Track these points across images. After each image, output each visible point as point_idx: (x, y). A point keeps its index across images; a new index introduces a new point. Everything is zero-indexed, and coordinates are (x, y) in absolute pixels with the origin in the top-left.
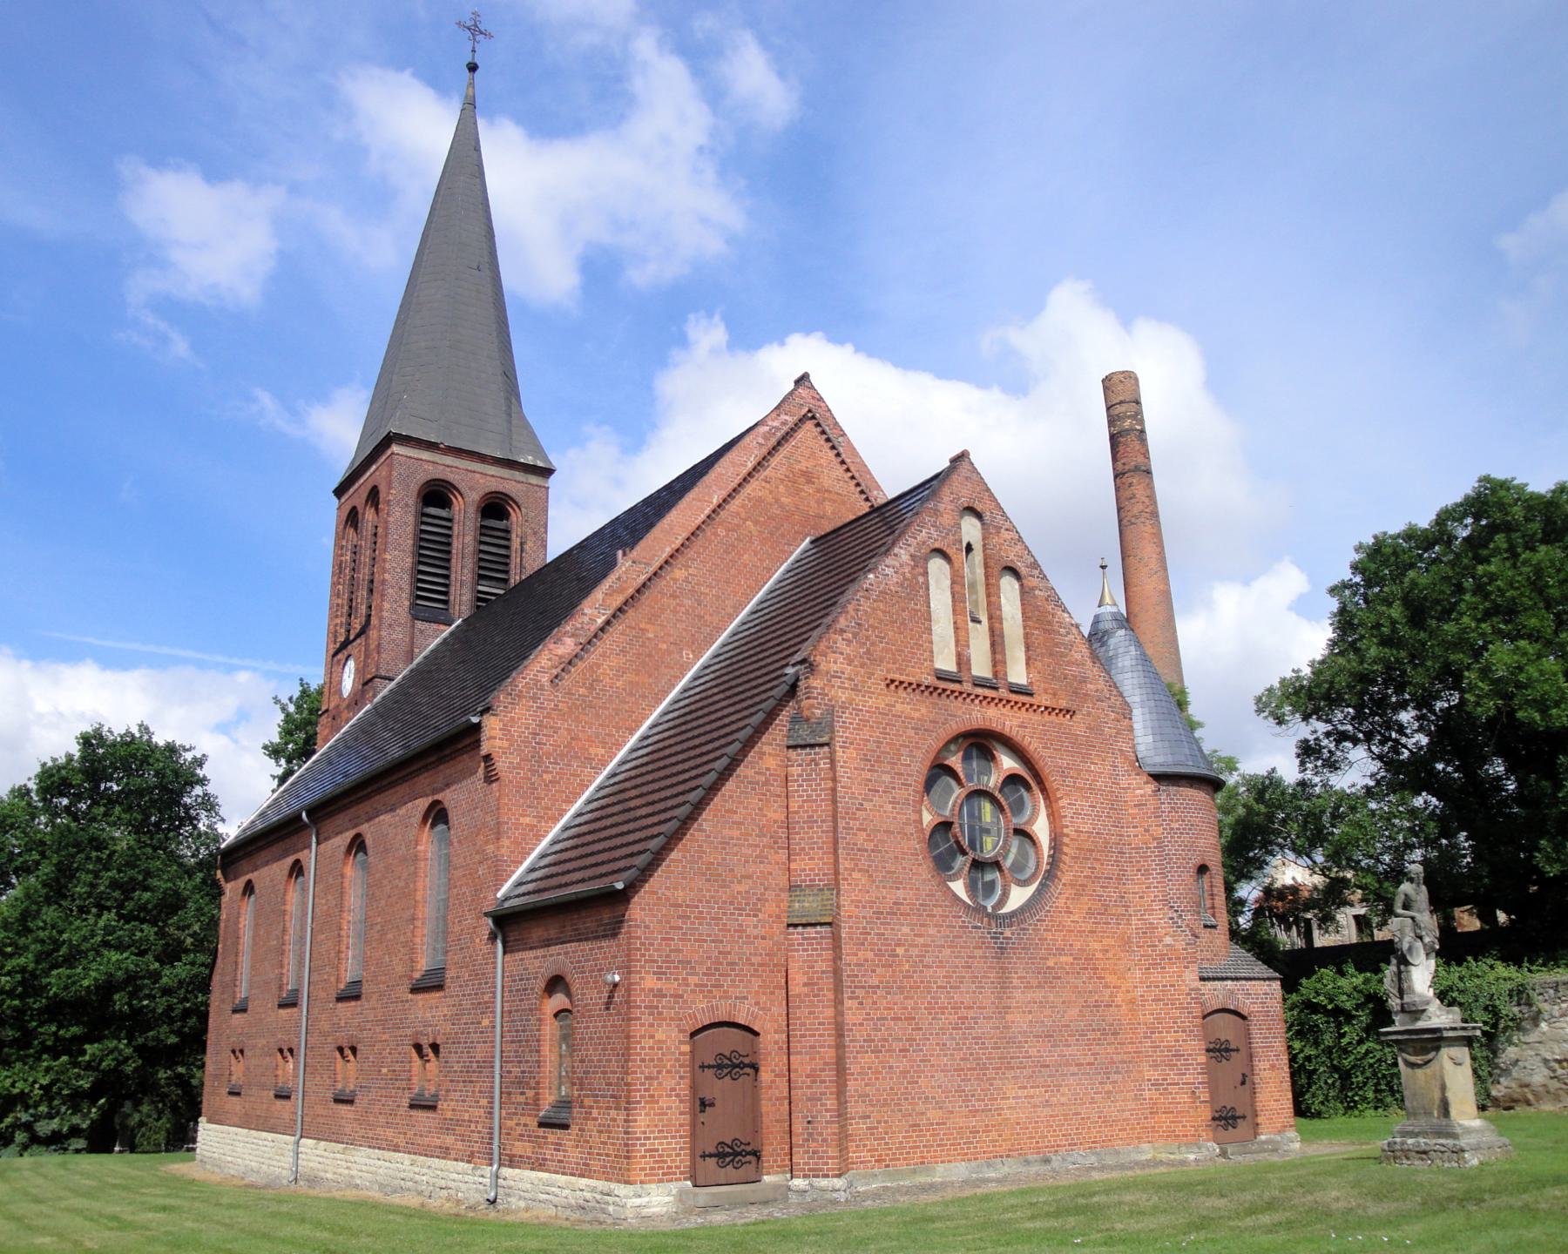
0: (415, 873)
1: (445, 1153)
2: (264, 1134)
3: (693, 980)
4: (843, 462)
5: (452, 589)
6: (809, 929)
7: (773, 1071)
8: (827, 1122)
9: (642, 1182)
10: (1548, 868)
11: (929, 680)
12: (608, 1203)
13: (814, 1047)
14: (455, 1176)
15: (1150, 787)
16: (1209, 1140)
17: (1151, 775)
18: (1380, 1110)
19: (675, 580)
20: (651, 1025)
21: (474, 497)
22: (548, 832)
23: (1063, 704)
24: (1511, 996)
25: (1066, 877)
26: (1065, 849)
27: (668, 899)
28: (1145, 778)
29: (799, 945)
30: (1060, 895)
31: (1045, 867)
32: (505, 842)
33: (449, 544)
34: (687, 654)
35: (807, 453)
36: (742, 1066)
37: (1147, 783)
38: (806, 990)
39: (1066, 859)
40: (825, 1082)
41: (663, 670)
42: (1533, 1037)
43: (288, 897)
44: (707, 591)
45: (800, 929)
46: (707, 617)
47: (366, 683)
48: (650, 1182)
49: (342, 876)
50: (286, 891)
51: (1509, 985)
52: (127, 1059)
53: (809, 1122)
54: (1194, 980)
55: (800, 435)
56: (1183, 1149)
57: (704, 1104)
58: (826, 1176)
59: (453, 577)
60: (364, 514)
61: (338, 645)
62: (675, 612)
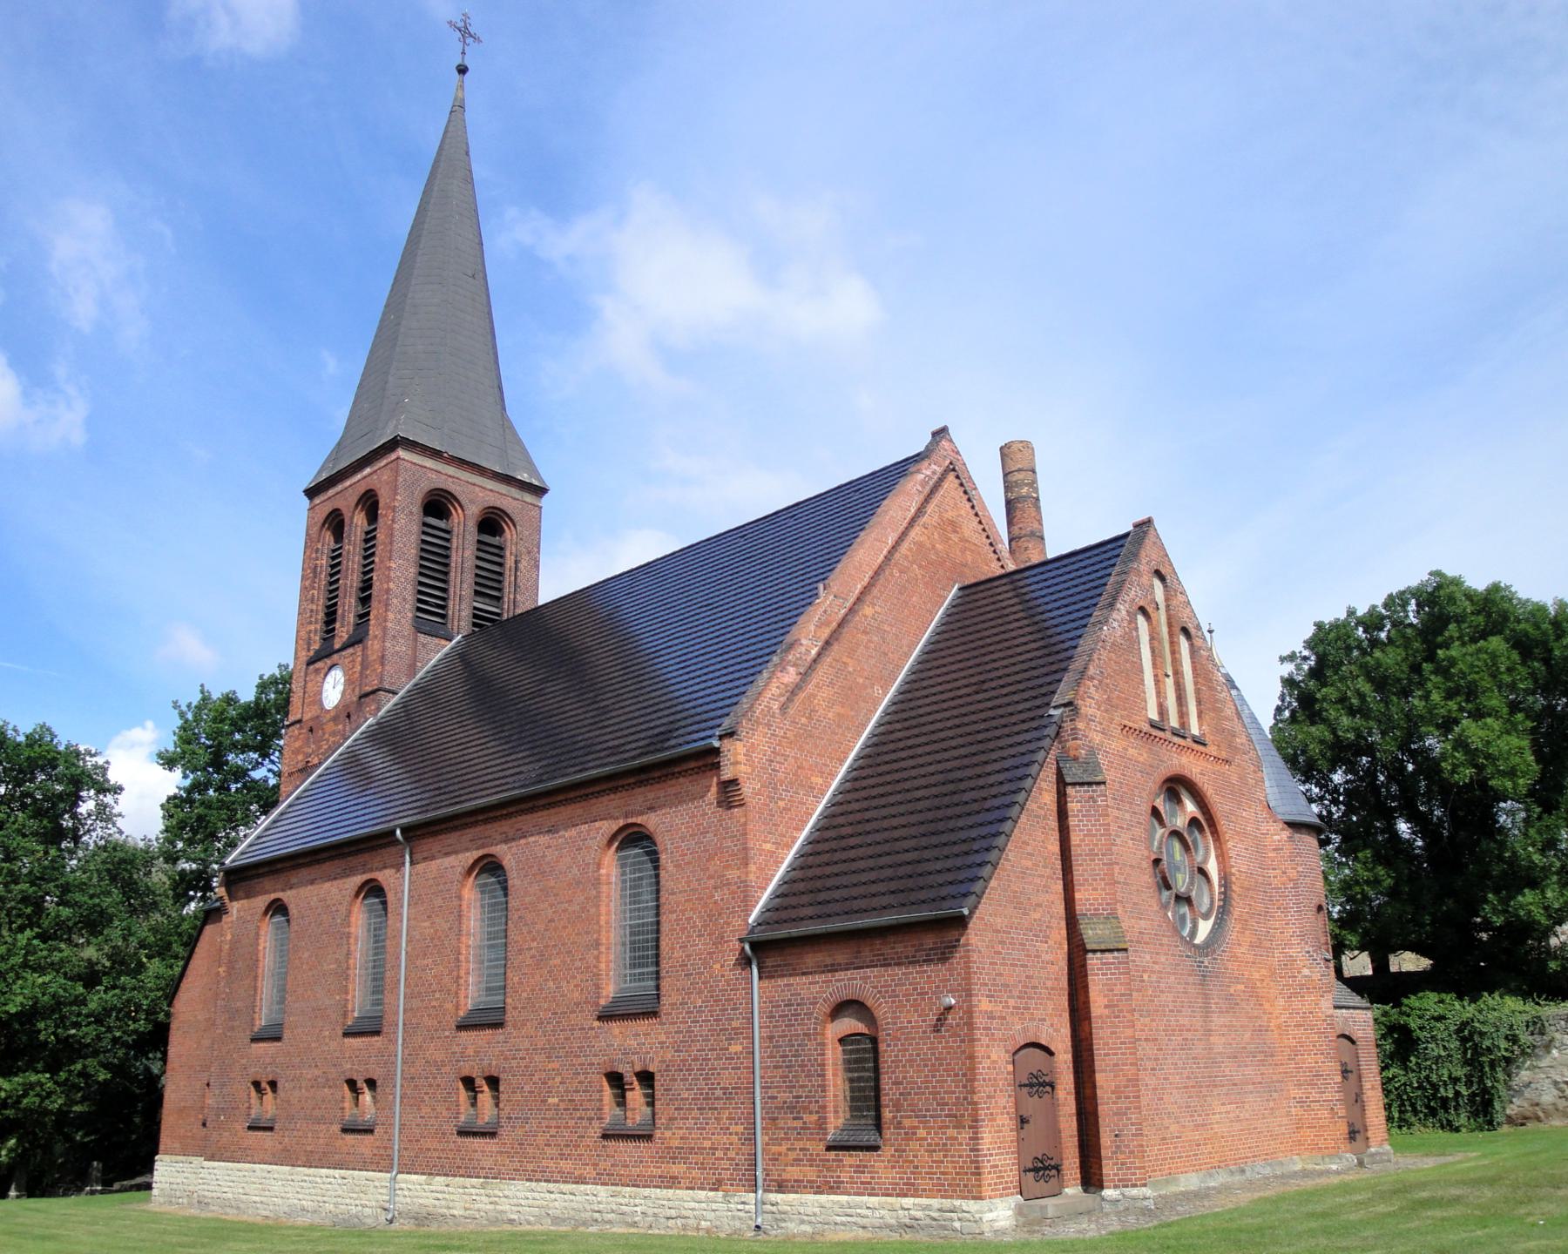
0: (598, 896)
1: (672, 1182)
2: (324, 1171)
3: (1012, 1002)
4: (976, 515)
5: (451, 603)
6: (1107, 955)
7: (1065, 1089)
8: (1133, 1135)
9: (990, 1198)
10: (1495, 919)
11: (1146, 728)
12: (952, 1220)
13: (1117, 1065)
14: (693, 1205)
15: (1286, 833)
16: (1347, 1152)
17: (1286, 823)
18: (1404, 1129)
19: (866, 616)
20: (988, 1046)
21: (473, 511)
22: (783, 859)
23: (1224, 755)
24: (1527, 1026)
25: (1236, 912)
26: (1234, 887)
27: (991, 925)
28: (1281, 825)
29: (1098, 969)
30: (1233, 925)
31: (1217, 903)
32: (752, 868)
33: (447, 557)
34: (878, 690)
35: (951, 503)
36: (1044, 1084)
37: (1283, 829)
38: (1107, 1012)
39: (1235, 896)
40: (1128, 1097)
41: (862, 705)
42: (1544, 1063)
43: (353, 919)
44: (888, 629)
45: (1099, 955)
46: (890, 654)
47: (361, 697)
48: (995, 1197)
49: (460, 898)
50: (350, 912)
51: (1526, 1017)
52: (49, 1094)
53: (1116, 1136)
54: (1329, 1008)
55: (946, 485)
56: (1327, 1160)
57: (1023, 1121)
58: (1135, 1186)
59: (451, 590)
60: (352, 518)
61: (312, 653)
62: (867, 647)
